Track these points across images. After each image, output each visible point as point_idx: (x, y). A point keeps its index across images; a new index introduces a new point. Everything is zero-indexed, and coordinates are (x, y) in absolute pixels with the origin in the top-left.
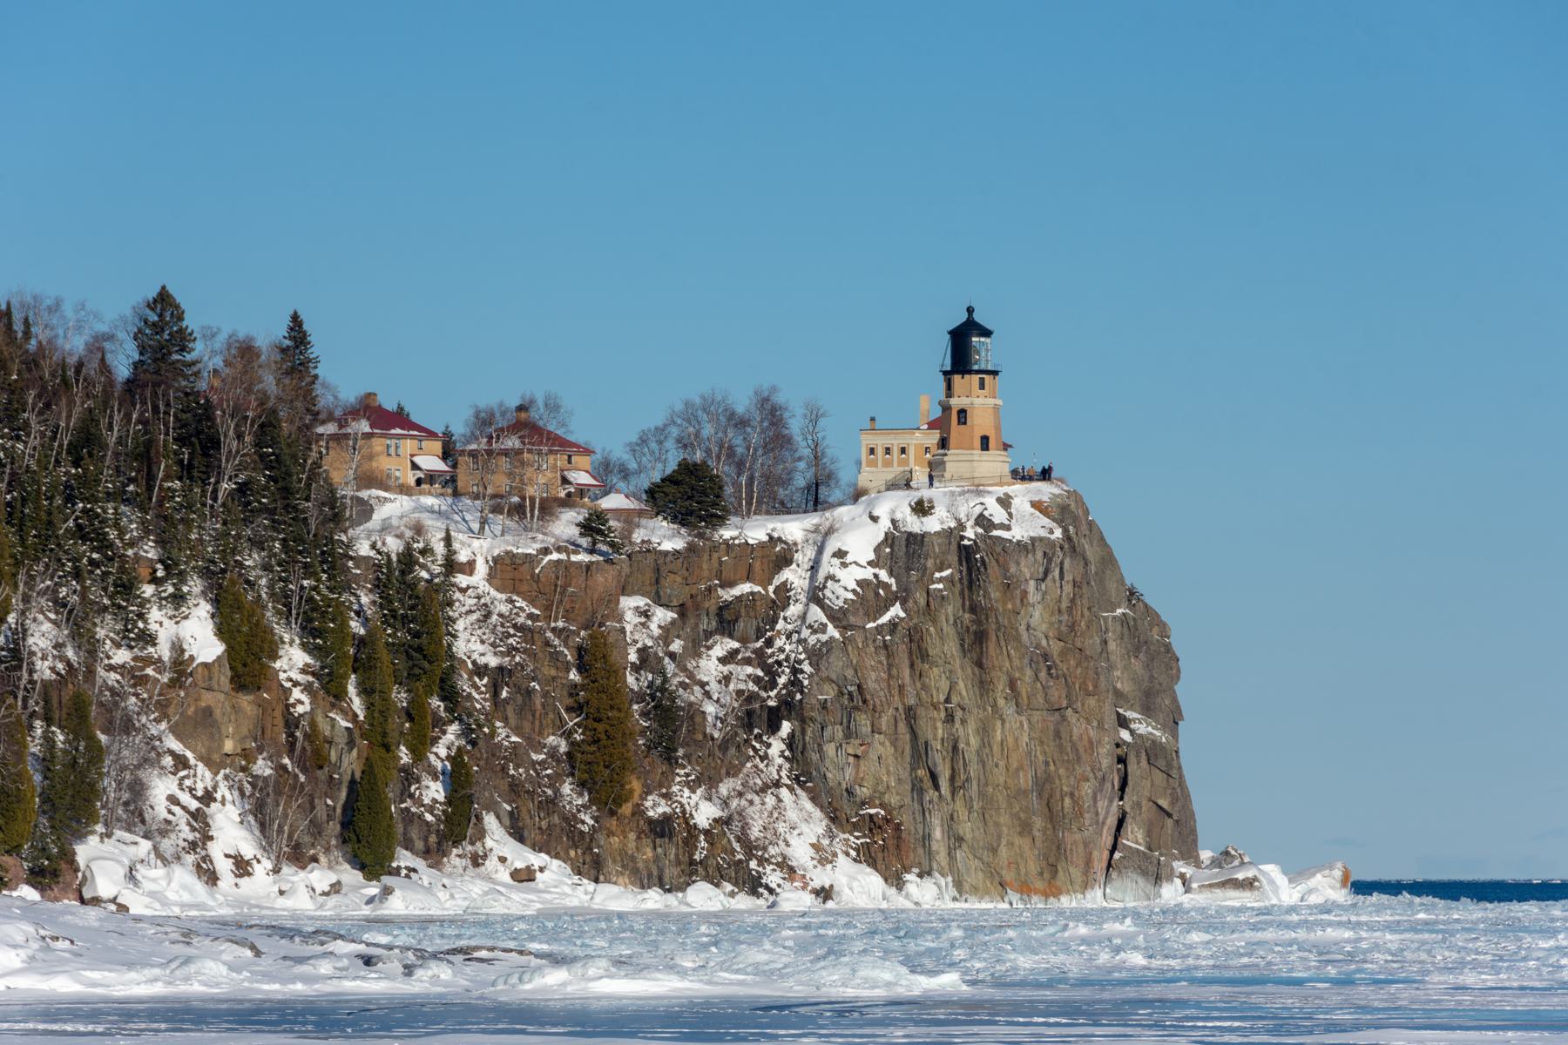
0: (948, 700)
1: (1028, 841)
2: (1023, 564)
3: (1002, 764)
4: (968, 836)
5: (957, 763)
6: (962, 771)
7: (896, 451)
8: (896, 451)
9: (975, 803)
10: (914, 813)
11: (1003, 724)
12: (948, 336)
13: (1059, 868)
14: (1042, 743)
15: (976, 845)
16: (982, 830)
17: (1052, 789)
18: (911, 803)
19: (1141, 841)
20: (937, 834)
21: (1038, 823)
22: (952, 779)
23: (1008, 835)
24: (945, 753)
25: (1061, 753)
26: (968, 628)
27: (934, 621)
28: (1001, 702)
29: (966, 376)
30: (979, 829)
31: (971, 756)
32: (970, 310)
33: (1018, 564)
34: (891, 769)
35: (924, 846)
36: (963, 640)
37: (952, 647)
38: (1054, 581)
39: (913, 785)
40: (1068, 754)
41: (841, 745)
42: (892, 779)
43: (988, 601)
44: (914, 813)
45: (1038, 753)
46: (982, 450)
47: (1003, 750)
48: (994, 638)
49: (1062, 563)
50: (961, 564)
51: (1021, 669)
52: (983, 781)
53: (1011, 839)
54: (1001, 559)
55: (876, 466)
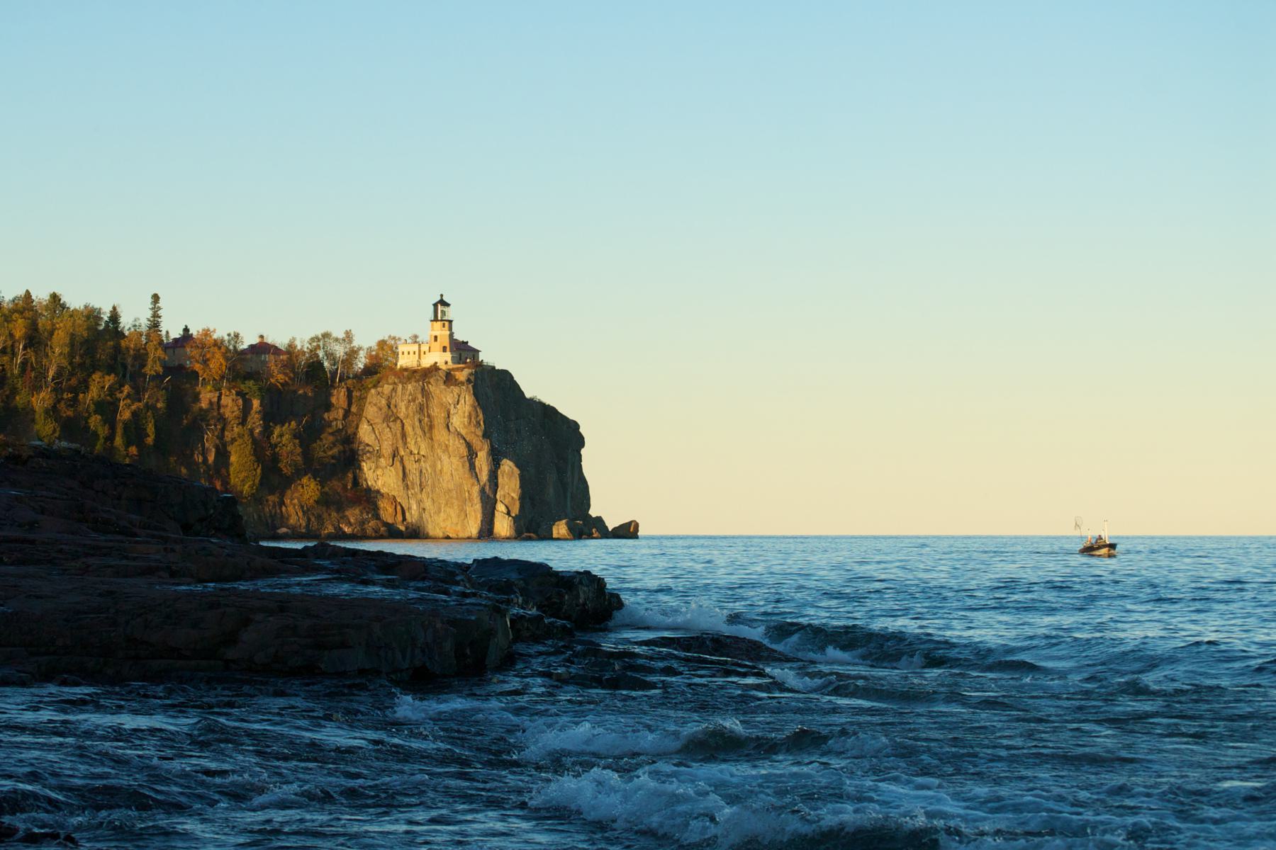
0: (418, 453)
7: (412, 353)
8: (412, 353)
21: (456, 502)
32: (442, 296)
51: (449, 440)
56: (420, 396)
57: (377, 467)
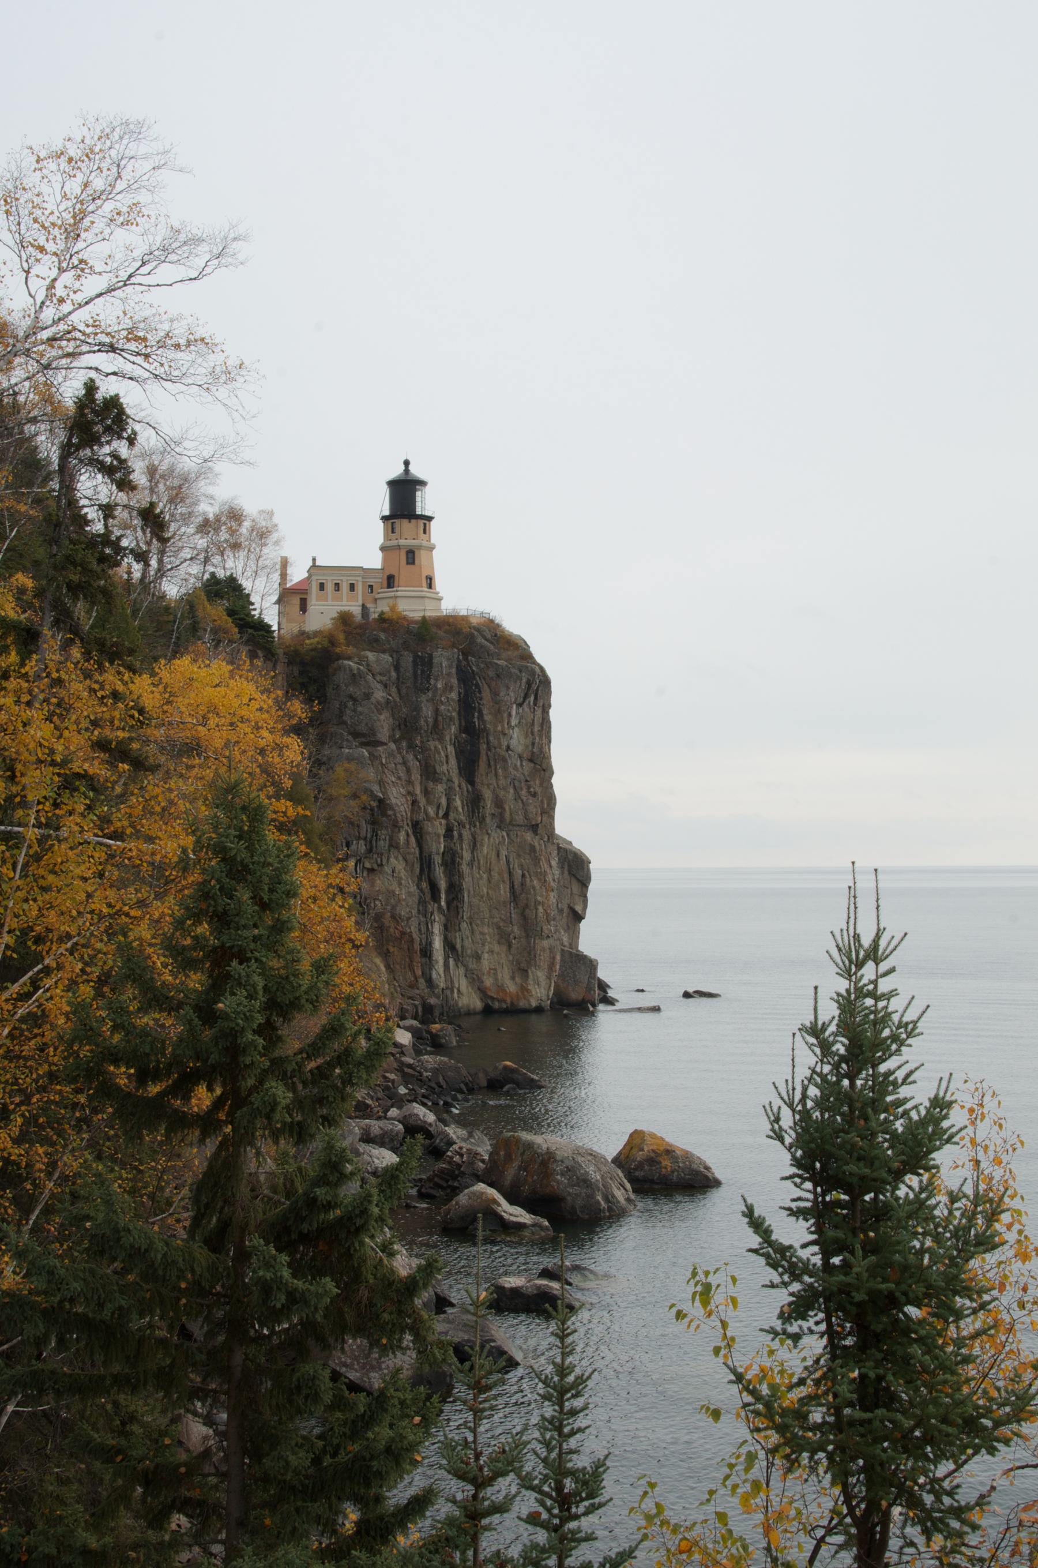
0: (446, 816)
1: (504, 948)
3: (485, 876)
7: (345, 588)
8: (345, 588)
12: (386, 486)
14: (519, 856)
17: (527, 899)
20: (438, 944)
27: (441, 739)
28: (488, 820)
32: (407, 463)
33: (508, 688)
42: (403, 892)
50: (460, 687)
54: (493, 684)
56: (454, 681)
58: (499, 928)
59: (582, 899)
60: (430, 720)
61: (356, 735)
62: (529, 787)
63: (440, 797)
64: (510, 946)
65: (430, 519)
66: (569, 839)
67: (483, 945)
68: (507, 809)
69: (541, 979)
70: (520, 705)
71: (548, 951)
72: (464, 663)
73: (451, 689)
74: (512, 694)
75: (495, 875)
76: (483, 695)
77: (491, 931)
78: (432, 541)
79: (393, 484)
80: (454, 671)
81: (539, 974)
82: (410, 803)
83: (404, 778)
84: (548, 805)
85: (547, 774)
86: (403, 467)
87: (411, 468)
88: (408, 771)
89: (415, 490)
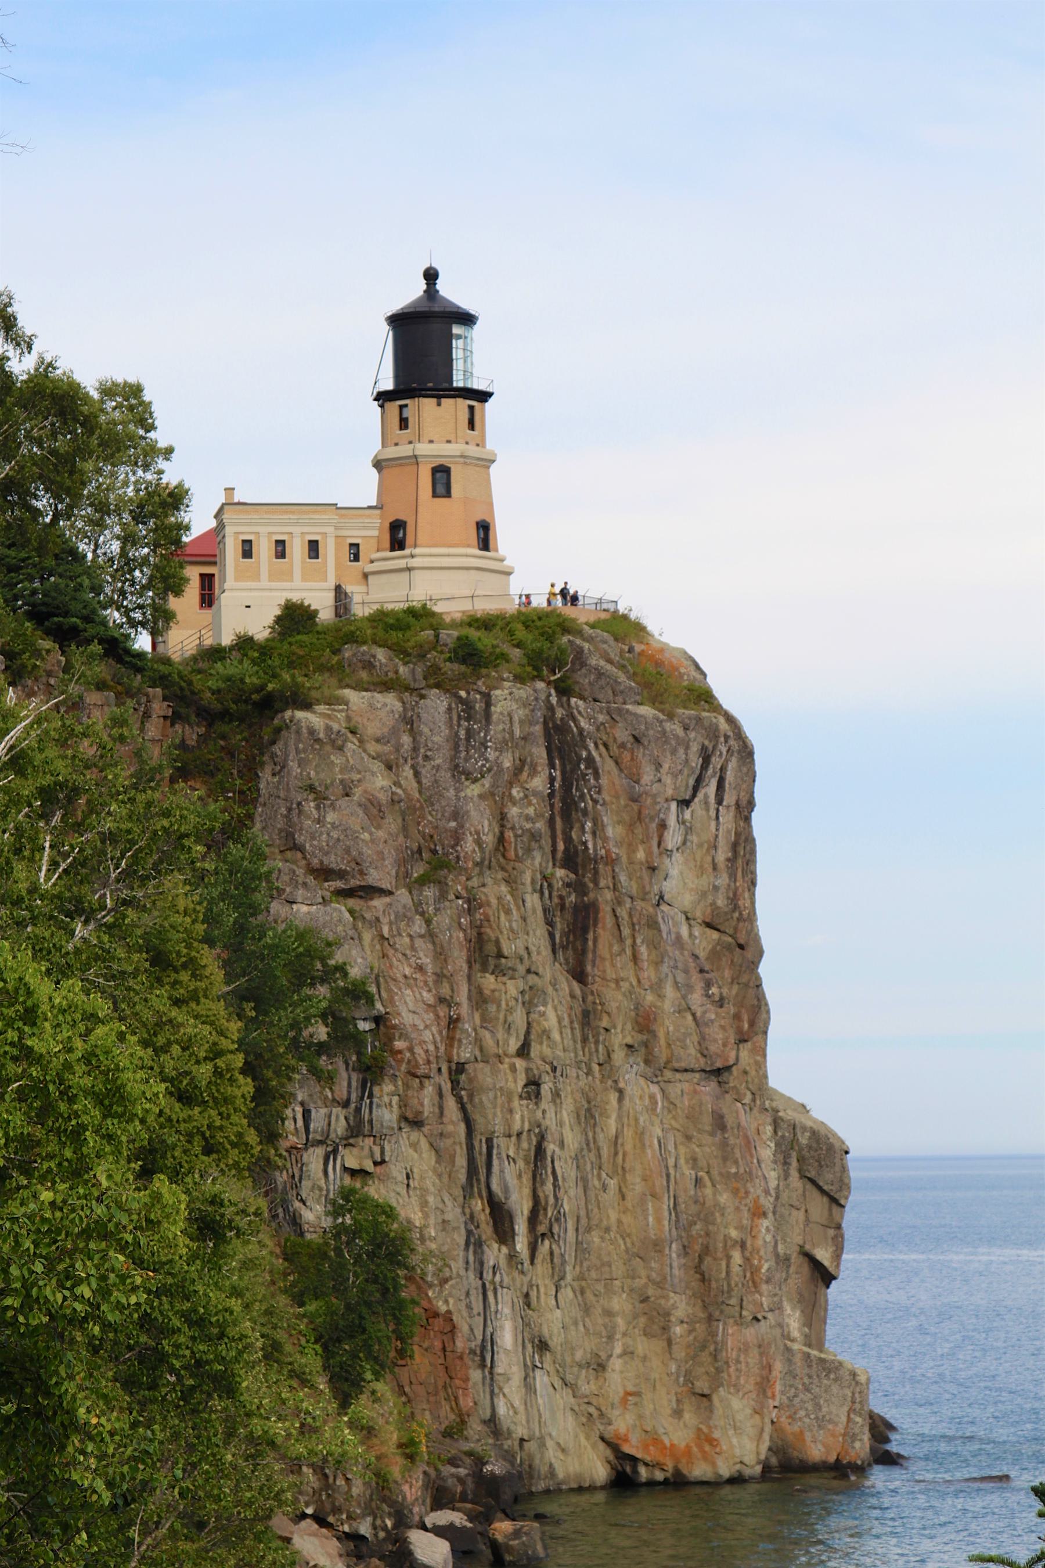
0: (523, 1051)
1: (659, 1345)
2: (666, 766)
3: (612, 1183)
4: (555, 1342)
5: (543, 1183)
6: (551, 1200)
7: (297, 550)
8: (297, 550)
9: (568, 1268)
10: (468, 1294)
11: (620, 1100)
13: (715, 1399)
14: (688, 1138)
15: (568, 1360)
16: (581, 1328)
17: (707, 1234)
18: (462, 1272)
19: (796, 1334)
20: (507, 1337)
21: (681, 1306)
22: (533, 1220)
23: (624, 1334)
24: (521, 1164)
25: (725, 1159)
26: (561, 897)
29: (443, 400)
30: (576, 1323)
31: (565, 1169)
32: (431, 276)
33: (658, 766)
34: (431, 1199)
35: (482, 1365)
36: (550, 923)
37: (538, 938)
38: (706, 803)
39: (469, 1233)
40: (736, 1162)
41: (335, 1152)
42: (432, 1221)
43: (599, 843)
44: (468, 1294)
45: (682, 1161)
46: (481, 549)
47: (616, 1154)
48: (609, 921)
49: (723, 769)
50: (552, 765)
51: (657, 988)
52: (584, 1221)
53: (630, 1342)
54: (626, 756)
55: (257, 577)
56: (539, 753)
57: (356, 1130)
58: (645, 1300)
59: (831, 1232)
60: (489, 839)
61: (324, 873)
62: (708, 984)
63: (510, 1010)
64: (669, 1342)
65: (483, 396)
66: (799, 1099)
67: (610, 1338)
68: (661, 1034)
69: (739, 1417)
70: (685, 803)
71: (756, 1351)
72: (560, 713)
73: (534, 772)
74: (668, 780)
75: (636, 1185)
76: (604, 781)
77: (628, 1307)
78: (490, 445)
79: (399, 321)
80: (538, 729)
81: (736, 1403)
82: (444, 1023)
83: (430, 969)
84: (752, 1024)
85: (749, 954)
86: (422, 285)
87: (441, 285)
88: (441, 955)
89: (449, 337)
